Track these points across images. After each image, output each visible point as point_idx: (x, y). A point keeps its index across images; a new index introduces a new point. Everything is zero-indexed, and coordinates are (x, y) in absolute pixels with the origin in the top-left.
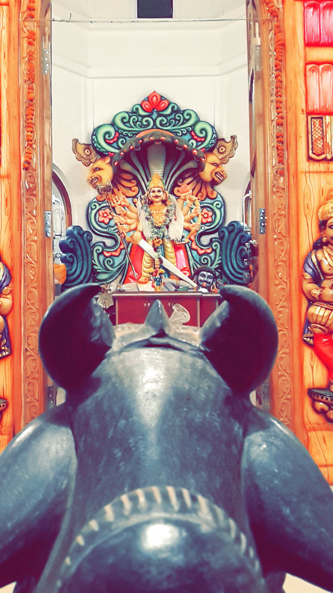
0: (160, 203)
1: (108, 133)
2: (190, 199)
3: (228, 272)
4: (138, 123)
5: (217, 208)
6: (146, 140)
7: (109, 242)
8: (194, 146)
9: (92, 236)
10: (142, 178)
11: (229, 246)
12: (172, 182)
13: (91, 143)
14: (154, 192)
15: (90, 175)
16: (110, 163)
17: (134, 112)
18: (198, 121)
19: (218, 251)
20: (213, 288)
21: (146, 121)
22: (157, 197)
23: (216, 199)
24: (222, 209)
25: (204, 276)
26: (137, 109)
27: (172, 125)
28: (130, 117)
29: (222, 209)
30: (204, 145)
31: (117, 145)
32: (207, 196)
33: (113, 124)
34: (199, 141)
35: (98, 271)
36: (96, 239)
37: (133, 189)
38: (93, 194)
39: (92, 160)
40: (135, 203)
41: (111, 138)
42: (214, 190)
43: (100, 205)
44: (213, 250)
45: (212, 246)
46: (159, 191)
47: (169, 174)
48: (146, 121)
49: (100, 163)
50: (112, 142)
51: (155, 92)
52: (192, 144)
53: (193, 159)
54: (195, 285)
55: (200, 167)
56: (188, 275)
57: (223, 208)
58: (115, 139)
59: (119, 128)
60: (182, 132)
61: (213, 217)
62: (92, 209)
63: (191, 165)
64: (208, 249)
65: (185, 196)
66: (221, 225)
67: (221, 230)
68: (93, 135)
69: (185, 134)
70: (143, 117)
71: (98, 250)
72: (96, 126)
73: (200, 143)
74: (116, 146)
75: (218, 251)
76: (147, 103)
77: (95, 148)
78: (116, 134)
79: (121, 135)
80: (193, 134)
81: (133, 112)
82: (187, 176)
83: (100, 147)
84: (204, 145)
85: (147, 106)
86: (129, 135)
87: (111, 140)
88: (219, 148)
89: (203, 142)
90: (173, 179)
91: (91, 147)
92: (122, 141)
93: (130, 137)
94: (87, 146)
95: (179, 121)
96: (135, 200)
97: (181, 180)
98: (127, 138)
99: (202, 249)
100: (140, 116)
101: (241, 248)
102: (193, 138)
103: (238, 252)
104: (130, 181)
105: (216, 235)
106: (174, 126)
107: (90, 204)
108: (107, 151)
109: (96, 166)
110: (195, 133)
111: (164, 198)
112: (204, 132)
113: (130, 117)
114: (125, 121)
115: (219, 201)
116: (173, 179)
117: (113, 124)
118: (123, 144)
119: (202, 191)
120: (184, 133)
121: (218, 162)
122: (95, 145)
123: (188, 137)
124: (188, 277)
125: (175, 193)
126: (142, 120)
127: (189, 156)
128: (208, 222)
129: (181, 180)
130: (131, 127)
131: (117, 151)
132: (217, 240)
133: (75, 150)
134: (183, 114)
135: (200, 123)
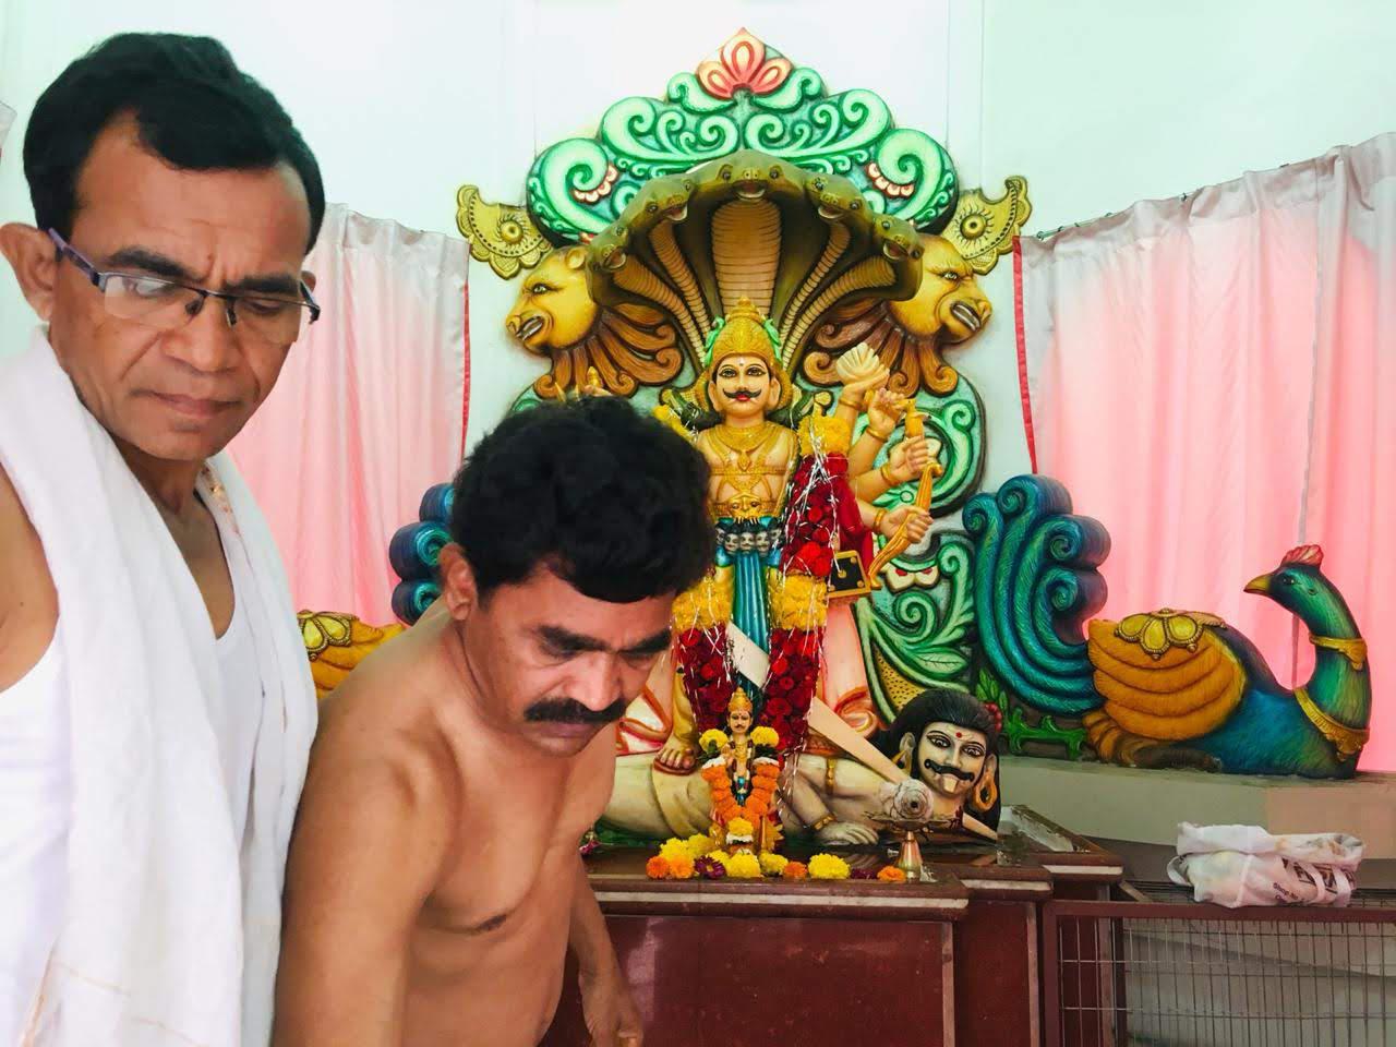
0: (758, 421)
2: (880, 407)
3: (1001, 662)
5: (955, 425)
10: (694, 318)
11: (1005, 568)
13: (524, 203)
14: (731, 373)
19: (961, 577)
20: (984, 794)
22: (742, 395)
23: (955, 397)
24: (976, 431)
25: (944, 743)
26: (682, 88)
28: (657, 118)
29: (976, 431)
30: (914, 208)
31: (613, 209)
32: (923, 386)
34: (894, 198)
37: (658, 356)
41: (591, 185)
42: (944, 363)
44: (942, 575)
45: (938, 562)
46: (752, 372)
47: (788, 308)
48: (711, 130)
50: (592, 198)
53: (881, 254)
55: (905, 284)
56: (867, 732)
57: (977, 423)
58: (606, 190)
60: (834, 164)
63: (877, 273)
64: (927, 571)
65: (863, 395)
66: (969, 487)
67: (973, 505)
68: (531, 175)
72: (541, 148)
73: (894, 205)
74: (609, 214)
75: (961, 577)
78: (607, 174)
81: (671, 101)
82: (850, 313)
83: (550, 213)
84: (914, 208)
86: (653, 173)
87: (590, 192)
89: (908, 199)
90: (802, 327)
91: (522, 216)
95: (825, 127)
97: (830, 329)
99: (901, 572)
100: (692, 112)
101: (1054, 574)
103: (1042, 589)
104: (651, 330)
105: (955, 522)
106: (807, 145)
110: (878, 169)
111: (773, 402)
113: (657, 118)
115: (966, 403)
119: (903, 368)
120: (841, 168)
121: (957, 265)
122: (538, 207)
124: (873, 739)
125: (809, 373)
126: (698, 126)
127: (864, 241)
129: (830, 329)
130: (663, 149)
132: (956, 538)
133: (467, 223)
134: (838, 106)
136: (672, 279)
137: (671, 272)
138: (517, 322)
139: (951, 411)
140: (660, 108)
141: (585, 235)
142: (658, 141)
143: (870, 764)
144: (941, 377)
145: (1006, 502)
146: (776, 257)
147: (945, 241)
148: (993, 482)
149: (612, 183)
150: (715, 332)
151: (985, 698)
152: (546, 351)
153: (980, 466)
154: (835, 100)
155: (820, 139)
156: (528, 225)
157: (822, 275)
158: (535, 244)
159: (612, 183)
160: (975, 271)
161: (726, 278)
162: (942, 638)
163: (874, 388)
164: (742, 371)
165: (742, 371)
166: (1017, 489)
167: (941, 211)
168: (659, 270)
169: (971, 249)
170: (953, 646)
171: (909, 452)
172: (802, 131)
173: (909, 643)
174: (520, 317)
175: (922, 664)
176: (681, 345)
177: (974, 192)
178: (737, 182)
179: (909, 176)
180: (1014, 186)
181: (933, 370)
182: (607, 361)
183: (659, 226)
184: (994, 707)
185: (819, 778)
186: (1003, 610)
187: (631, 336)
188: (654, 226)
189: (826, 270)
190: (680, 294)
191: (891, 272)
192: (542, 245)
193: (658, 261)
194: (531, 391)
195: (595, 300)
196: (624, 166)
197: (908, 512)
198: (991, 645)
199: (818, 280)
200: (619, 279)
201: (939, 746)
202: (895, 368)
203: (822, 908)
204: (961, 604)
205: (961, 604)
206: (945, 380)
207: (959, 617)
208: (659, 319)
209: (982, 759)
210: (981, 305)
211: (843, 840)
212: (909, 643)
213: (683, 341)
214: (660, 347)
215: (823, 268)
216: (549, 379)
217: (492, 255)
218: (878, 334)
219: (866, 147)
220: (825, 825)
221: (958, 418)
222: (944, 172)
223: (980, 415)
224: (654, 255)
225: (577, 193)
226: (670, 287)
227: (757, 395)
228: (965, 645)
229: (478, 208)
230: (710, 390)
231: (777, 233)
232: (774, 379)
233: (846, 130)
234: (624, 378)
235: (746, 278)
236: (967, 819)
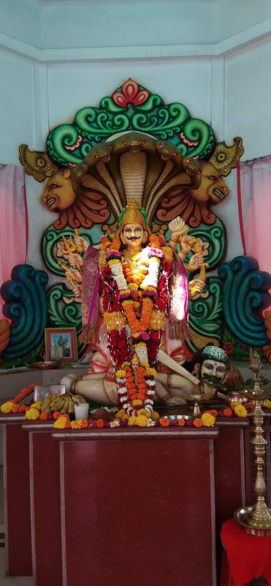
1: (68, 137)
2: (187, 242)
4: (108, 122)
5: (216, 237)
6: (119, 146)
8: (184, 154)
9: (47, 278)
11: (234, 291)
12: (154, 203)
13: (46, 151)
14: (129, 230)
17: (103, 108)
18: (189, 118)
19: (217, 295)
23: (215, 225)
24: (223, 239)
26: (107, 103)
27: (154, 125)
28: (97, 115)
29: (223, 239)
31: (81, 153)
32: (202, 221)
35: (57, 323)
36: (53, 280)
37: (101, 213)
38: (50, 218)
40: (105, 232)
41: (72, 143)
42: (211, 212)
43: (58, 234)
44: (210, 294)
46: (137, 229)
47: (150, 192)
48: (119, 120)
50: (72, 149)
51: (130, 79)
52: (182, 150)
54: (197, 381)
55: (195, 184)
56: (182, 363)
58: (78, 146)
59: (83, 130)
60: (167, 133)
61: (211, 250)
62: (48, 241)
63: (183, 179)
64: (204, 293)
65: (179, 237)
68: (48, 139)
69: (172, 137)
70: (115, 114)
71: (56, 295)
72: (51, 128)
73: (190, 149)
75: (217, 295)
76: (119, 94)
77: (51, 157)
79: (85, 140)
80: (183, 137)
82: (174, 193)
83: (57, 156)
85: (120, 99)
86: (96, 138)
87: (72, 146)
88: (218, 155)
89: (196, 148)
90: (156, 199)
91: (46, 157)
92: (87, 148)
93: (97, 142)
94: (39, 155)
95: (163, 118)
96: (106, 227)
98: (93, 143)
100: (111, 112)
102: (182, 142)
104: (98, 202)
105: (215, 273)
106: (157, 125)
107: (45, 233)
112: (197, 135)
113: (97, 115)
114: (91, 119)
117: (75, 124)
120: (170, 135)
123: (175, 141)
124: (183, 366)
127: (179, 168)
129: (166, 200)
130: (100, 128)
131: (79, 161)
134: (168, 110)
135: (193, 121)
136: (104, 181)
137: (104, 179)
138: (45, 200)
139: (213, 231)
140: (98, 111)
141: (70, 164)
142: (98, 125)
143: (184, 375)
144: (209, 218)
145: (234, 267)
146: (145, 173)
147: (211, 164)
148: (230, 257)
149: (80, 143)
150: (121, 214)
151: (226, 340)
152: (57, 210)
153: (224, 251)
154: (167, 107)
155: (162, 123)
156: (47, 159)
157: (163, 179)
158: (51, 167)
159: (80, 143)
160: (222, 175)
161: (126, 181)
162: (210, 318)
163: (183, 235)
164: (133, 229)
165: (133, 229)
166: (238, 262)
167: (209, 152)
168: (100, 179)
169: (221, 166)
170: (214, 321)
171: (196, 259)
172: (154, 120)
173: (199, 320)
174: (46, 197)
175: (203, 327)
176: (109, 208)
177: (222, 143)
178: (129, 146)
179: (196, 138)
180: (238, 141)
181: (206, 215)
182: (81, 214)
183: (100, 163)
184: (230, 343)
185: (165, 381)
186: (233, 307)
187: (89, 204)
188: (97, 163)
189: (164, 177)
190: (108, 188)
191: (190, 179)
192: (54, 168)
193: (100, 176)
194: (52, 227)
195: (75, 192)
196: (84, 135)
197: (196, 282)
198: (229, 321)
199: (162, 181)
200: (84, 184)
201: (209, 368)
203: (167, 436)
204: (217, 305)
205: (217, 305)
206: (211, 219)
207: (216, 310)
208: (100, 197)
209: (224, 373)
210: (225, 189)
211: (174, 404)
212: (199, 320)
213: (110, 206)
214: (101, 208)
215: (163, 176)
216: (59, 222)
217: (34, 172)
218: (185, 201)
219: (179, 126)
220: (167, 398)
221: (216, 233)
222: (210, 136)
223: (224, 231)
225: (66, 147)
226: (104, 185)
227: (140, 237)
228: (220, 320)
230: (121, 236)
231: (145, 164)
232: (146, 232)
233: (171, 120)
234: (88, 221)
235: (134, 181)
236: (219, 394)
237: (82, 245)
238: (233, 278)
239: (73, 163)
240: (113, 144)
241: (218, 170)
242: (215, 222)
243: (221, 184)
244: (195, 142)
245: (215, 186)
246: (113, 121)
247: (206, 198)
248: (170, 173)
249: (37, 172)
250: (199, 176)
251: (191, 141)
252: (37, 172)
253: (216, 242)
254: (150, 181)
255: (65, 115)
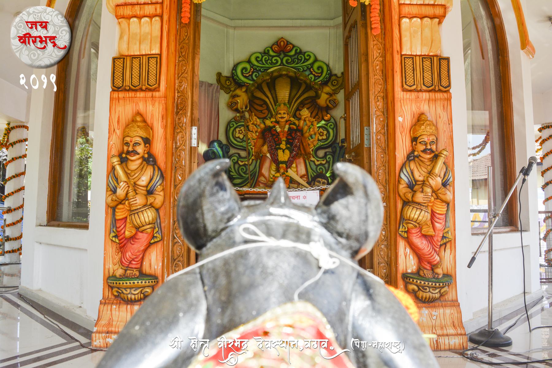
1: (245, 68)
2: (309, 121)
6: (276, 74)
7: (243, 154)
12: (295, 107)
14: (280, 114)
15: (231, 100)
16: (246, 92)
17: (265, 53)
18: (316, 60)
19: (331, 162)
21: (275, 60)
22: (282, 118)
24: (335, 129)
26: (268, 51)
28: (262, 57)
29: (335, 129)
30: (321, 79)
33: (249, 62)
39: (232, 89)
43: (236, 124)
44: (327, 162)
46: (284, 113)
48: (275, 60)
49: (238, 92)
50: (247, 75)
55: (318, 96)
59: (254, 65)
62: (230, 127)
63: (311, 93)
64: (323, 161)
67: (333, 146)
68: (233, 70)
69: (306, 71)
70: (273, 57)
71: (234, 160)
75: (331, 162)
77: (234, 80)
78: (251, 70)
80: (312, 70)
82: (307, 102)
84: (321, 79)
89: (319, 77)
90: (296, 105)
91: (231, 79)
92: (256, 75)
94: (227, 78)
95: (301, 60)
98: (260, 73)
99: (318, 161)
100: (271, 56)
102: (311, 73)
104: (261, 106)
105: (329, 150)
106: (297, 64)
107: (229, 123)
108: (245, 83)
109: (234, 93)
112: (320, 69)
113: (262, 57)
114: (259, 59)
116: (296, 105)
118: (256, 77)
121: (331, 92)
123: (307, 73)
124: (307, 183)
125: (297, 115)
127: (309, 87)
128: (323, 139)
130: (264, 64)
131: (251, 82)
133: (219, 81)
139: (329, 125)
179: (319, 71)
187: (256, 107)
190: (268, 97)
200: (255, 94)
202: (311, 113)
215: (300, 92)
219: (310, 64)
222: (328, 70)
223: (336, 125)
224: (262, 89)
229: (221, 78)
237: (256, 121)
238: (340, 151)
239: (247, 83)
240: (272, 72)
241: (333, 90)
242: (330, 119)
243: (334, 97)
244: (319, 73)
245: (331, 98)
246: (271, 60)
247: (325, 105)
248: (304, 90)
249: (226, 88)
250: (320, 92)
251: (317, 73)
252: (226, 88)
253: (331, 131)
254: (293, 94)
255: (244, 56)
